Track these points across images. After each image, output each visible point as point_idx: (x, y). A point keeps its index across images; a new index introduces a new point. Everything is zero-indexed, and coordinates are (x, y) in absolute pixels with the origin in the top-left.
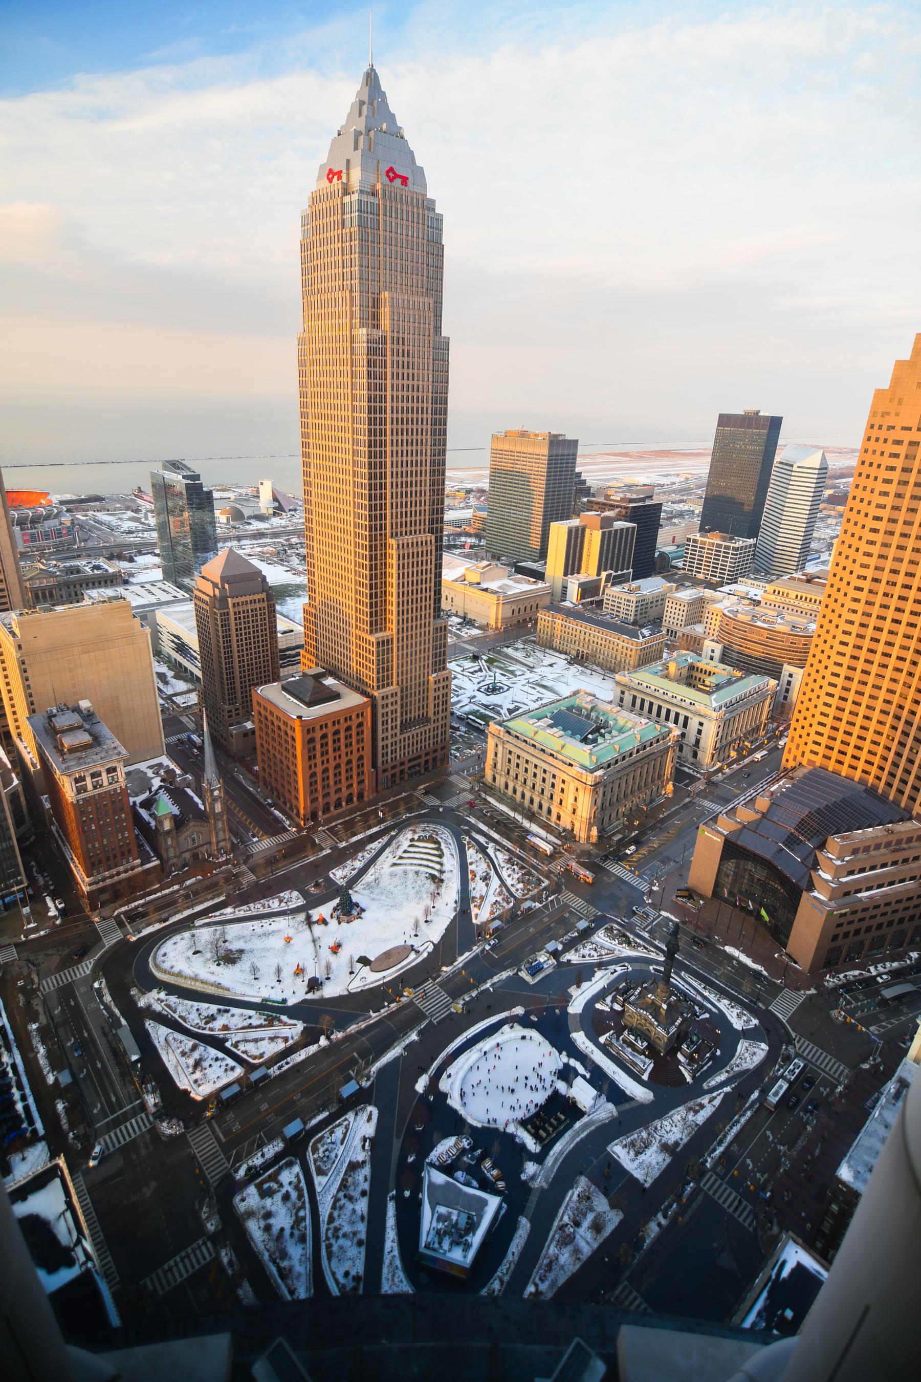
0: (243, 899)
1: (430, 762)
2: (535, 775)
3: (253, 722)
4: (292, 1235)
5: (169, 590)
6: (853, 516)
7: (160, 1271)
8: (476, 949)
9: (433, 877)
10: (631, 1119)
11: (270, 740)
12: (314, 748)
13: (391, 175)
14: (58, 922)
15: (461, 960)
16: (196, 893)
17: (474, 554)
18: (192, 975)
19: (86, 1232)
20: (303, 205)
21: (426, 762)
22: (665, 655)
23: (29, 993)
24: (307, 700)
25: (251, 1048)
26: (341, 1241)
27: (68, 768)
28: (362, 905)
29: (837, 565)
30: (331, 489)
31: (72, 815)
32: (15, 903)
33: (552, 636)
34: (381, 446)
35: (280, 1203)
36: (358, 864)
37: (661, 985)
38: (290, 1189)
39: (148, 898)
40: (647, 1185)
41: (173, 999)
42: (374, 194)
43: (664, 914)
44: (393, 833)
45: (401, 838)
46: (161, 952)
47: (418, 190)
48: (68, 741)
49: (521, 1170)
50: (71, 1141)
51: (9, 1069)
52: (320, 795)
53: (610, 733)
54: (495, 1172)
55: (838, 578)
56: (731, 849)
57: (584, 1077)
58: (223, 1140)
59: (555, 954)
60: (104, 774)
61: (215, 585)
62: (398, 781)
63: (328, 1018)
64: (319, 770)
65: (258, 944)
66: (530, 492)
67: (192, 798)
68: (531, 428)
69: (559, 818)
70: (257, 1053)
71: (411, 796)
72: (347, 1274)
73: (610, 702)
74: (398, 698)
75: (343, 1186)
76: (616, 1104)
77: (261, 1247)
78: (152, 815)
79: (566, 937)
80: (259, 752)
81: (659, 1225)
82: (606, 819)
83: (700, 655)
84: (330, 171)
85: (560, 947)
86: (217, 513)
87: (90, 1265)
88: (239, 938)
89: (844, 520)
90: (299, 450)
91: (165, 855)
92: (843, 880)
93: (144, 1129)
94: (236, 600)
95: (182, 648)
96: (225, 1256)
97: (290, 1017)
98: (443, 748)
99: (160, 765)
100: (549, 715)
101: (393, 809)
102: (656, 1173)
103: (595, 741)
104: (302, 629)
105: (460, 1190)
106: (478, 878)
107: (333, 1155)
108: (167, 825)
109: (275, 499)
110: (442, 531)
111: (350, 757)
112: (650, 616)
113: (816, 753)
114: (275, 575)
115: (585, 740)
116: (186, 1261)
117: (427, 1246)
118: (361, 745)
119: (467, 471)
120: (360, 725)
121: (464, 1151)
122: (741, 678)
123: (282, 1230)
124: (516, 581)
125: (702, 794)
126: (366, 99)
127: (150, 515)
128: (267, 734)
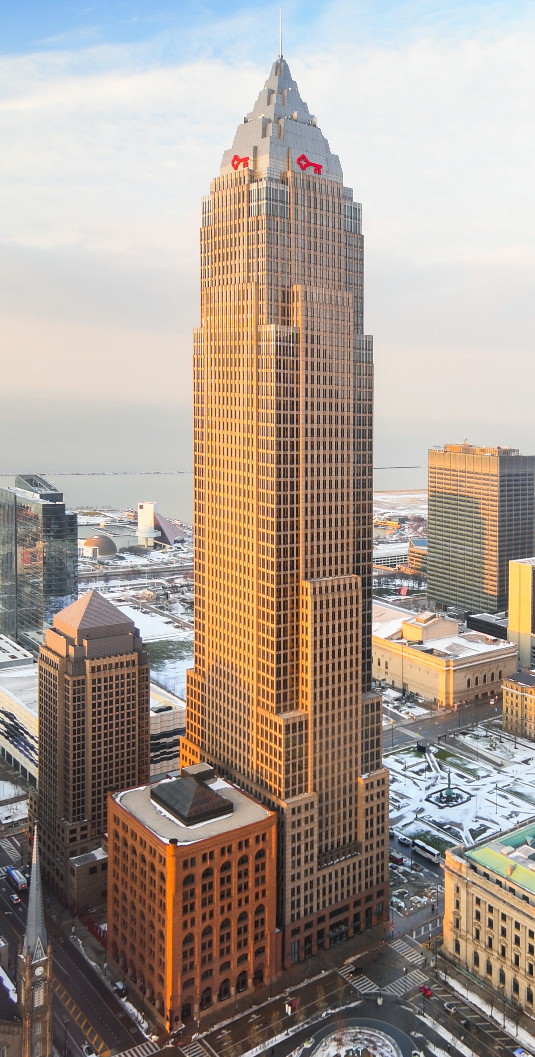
1: (363, 916)
3: (106, 850)
12: (192, 893)
17: (413, 602)
20: (206, 191)
42: (284, 181)
52: (197, 974)
61: (70, 641)
62: (315, 949)
66: (480, 522)
68: (475, 442)
71: (334, 976)
74: (315, 812)
80: (110, 899)
84: (236, 158)
94: (96, 663)
101: (306, 998)
104: (184, 706)
109: (157, 527)
110: (370, 572)
111: (244, 908)
114: (152, 628)
119: (399, 495)
120: (261, 854)
124: (471, 639)
126: (275, 88)
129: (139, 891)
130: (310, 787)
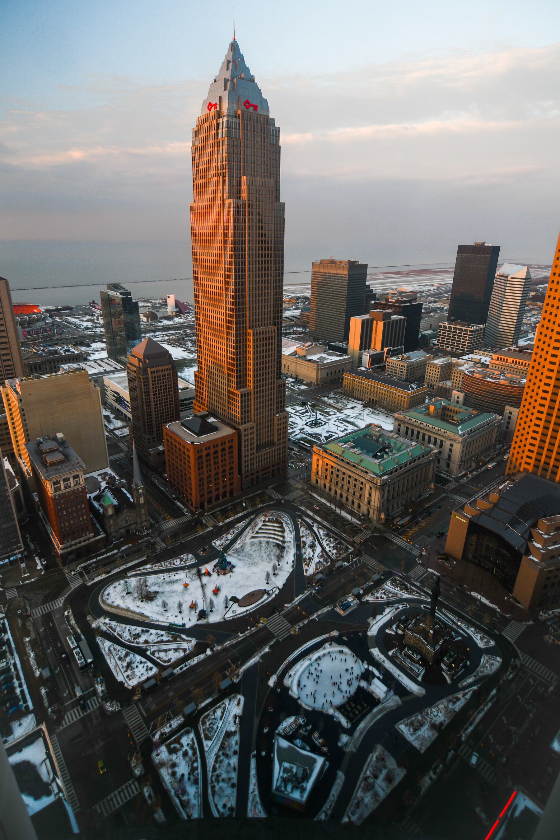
0: (158, 559)
2: (343, 479)
3: (164, 446)
4: (189, 779)
5: (112, 364)
6: (549, 309)
7: (105, 800)
8: (307, 593)
9: (278, 545)
10: (410, 706)
11: (174, 457)
12: (202, 463)
13: (247, 104)
14: (43, 573)
15: (297, 600)
16: (128, 555)
17: (302, 338)
18: (125, 607)
19: (59, 773)
20: (193, 124)
21: (273, 471)
22: (427, 401)
23: (25, 617)
24: (197, 432)
25: (162, 655)
26: (221, 784)
27: (49, 476)
28: (233, 563)
29: (539, 340)
30: (211, 299)
31: (52, 505)
32: (16, 560)
33: (353, 389)
34: (242, 272)
35: (181, 758)
36: (230, 537)
37: (429, 617)
38: (188, 748)
39: (98, 558)
40: (422, 752)
41: (113, 623)
43: (430, 570)
44: (252, 517)
45: (257, 520)
46: (106, 592)
47: (264, 113)
48: (50, 459)
49: (338, 739)
50: (49, 714)
51: (12, 667)
52: (205, 492)
53: (392, 451)
54: (321, 741)
55: (540, 349)
56: (474, 527)
57: (378, 678)
58: (145, 715)
59: (358, 596)
60: (71, 480)
61: (140, 360)
62: (255, 483)
63: (212, 636)
64: (205, 476)
65: (167, 588)
67: (125, 494)
68: (336, 258)
69: (359, 506)
70: (167, 659)
71: (264, 492)
72: (224, 806)
73: (391, 432)
74: (255, 430)
75: (222, 747)
76: (400, 697)
77: (169, 786)
78: (101, 505)
79: (366, 585)
80: (167, 465)
81: (431, 778)
82: (390, 508)
83: (450, 400)
84: (210, 104)
85: (361, 592)
86: (141, 315)
87: (61, 795)
88: (155, 584)
89: (543, 311)
90: (191, 275)
91: (109, 531)
92: (550, 548)
93: (95, 707)
95: (119, 399)
96: (146, 792)
97: (187, 636)
98: (284, 462)
99: (106, 474)
100: (352, 440)
101: (252, 501)
102: (428, 744)
103: (382, 457)
104: (194, 387)
105: (298, 752)
106: (307, 546)
107: (215, 727)
108: (110, 512)
110: (281, 324)
111: (224, 468)
112: (416, 375)
113: (529, 464)
114: (177, 353)
115: (375, 457)
116: (122, 794)
117: (278, 789)
118: (232, 460)
120: (231, 447)
121: (300, 726)
122: (477, 415)
123: (183, 775)
124: (329, 354)
125: (455, 491)
126: (231, 60)
127: (100, 317)
128: (172, 453)
129: (179, 462)
130: (253, 420)
